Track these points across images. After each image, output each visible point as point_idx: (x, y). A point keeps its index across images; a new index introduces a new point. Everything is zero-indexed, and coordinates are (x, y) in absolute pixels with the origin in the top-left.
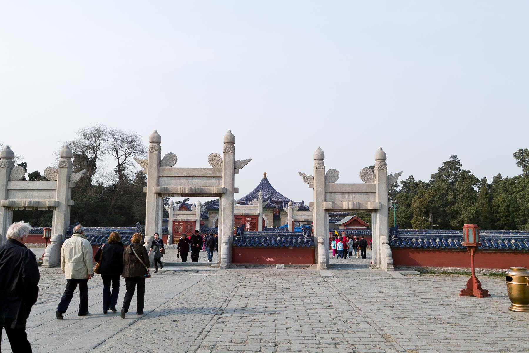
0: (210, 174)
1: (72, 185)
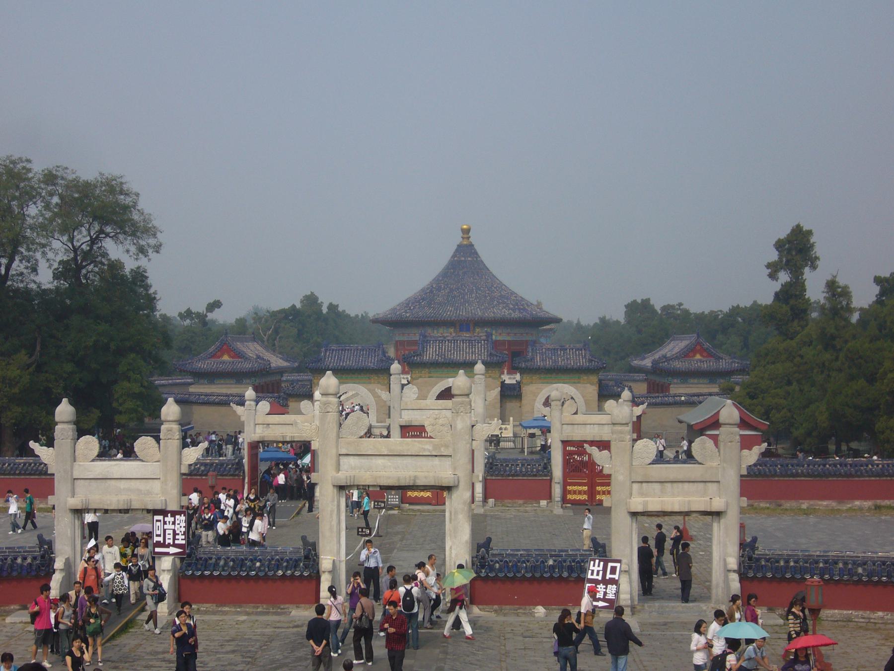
0: (429, 451)
1: (184, 470)
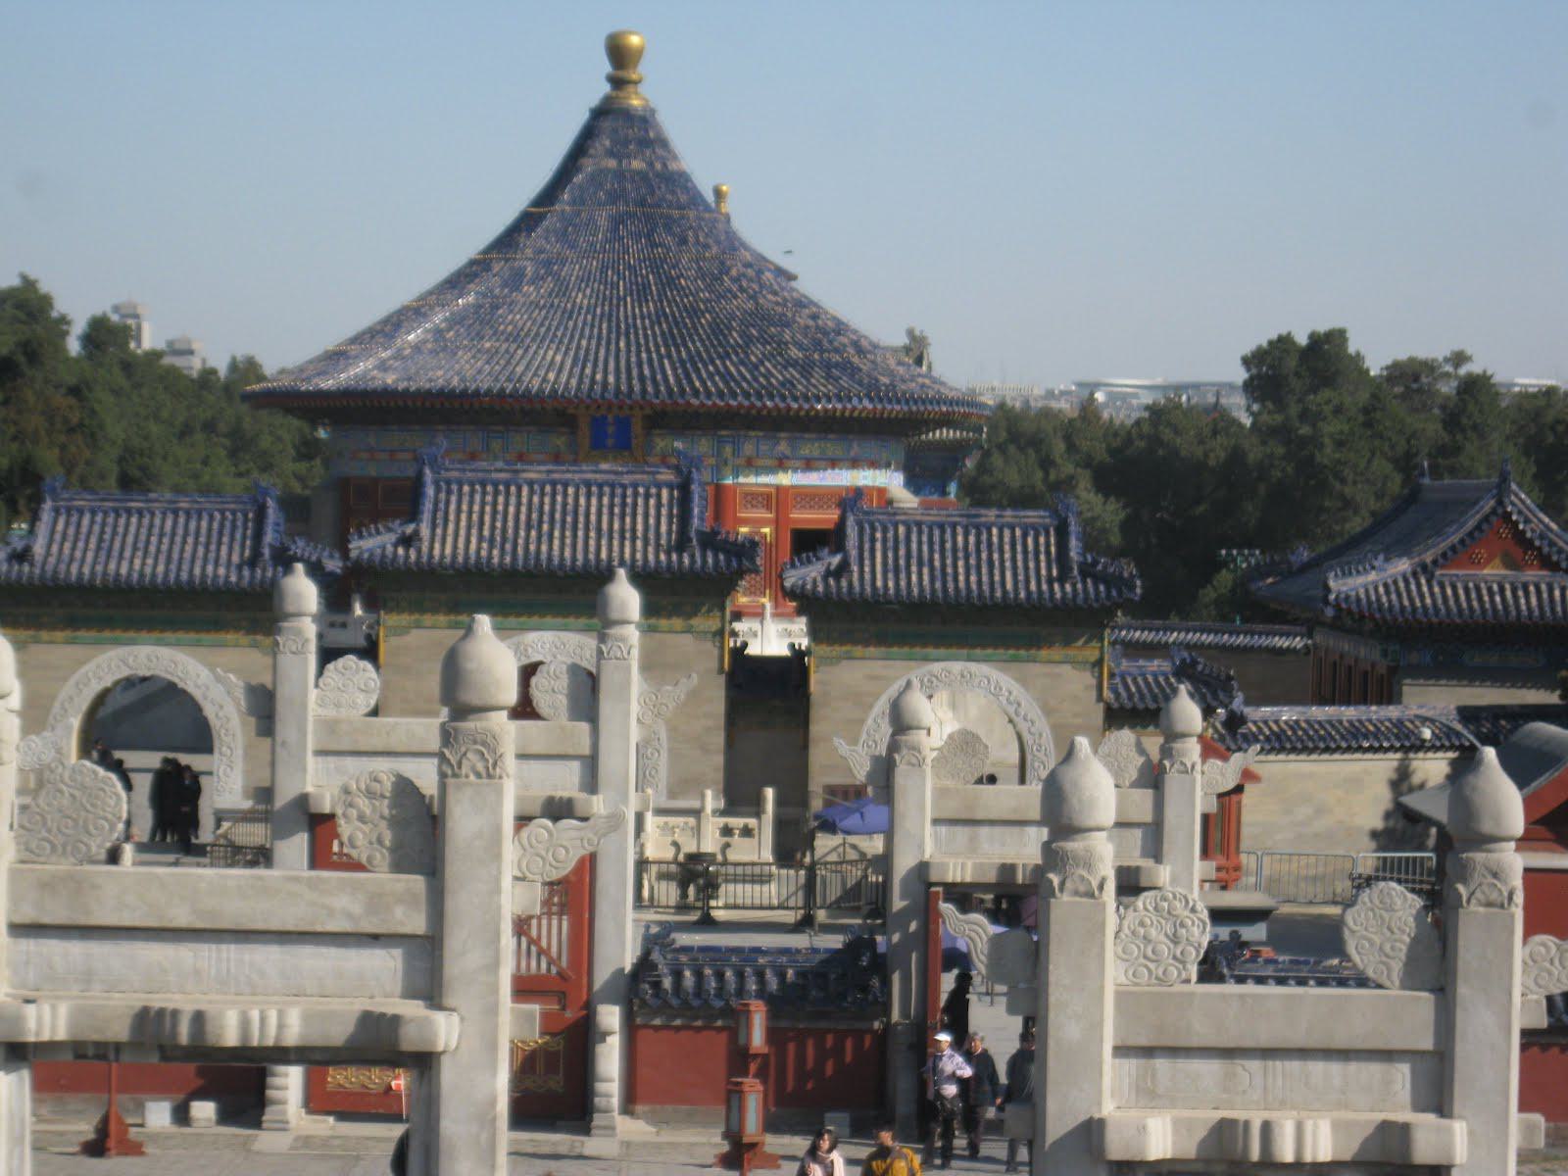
0: (349, 916)
